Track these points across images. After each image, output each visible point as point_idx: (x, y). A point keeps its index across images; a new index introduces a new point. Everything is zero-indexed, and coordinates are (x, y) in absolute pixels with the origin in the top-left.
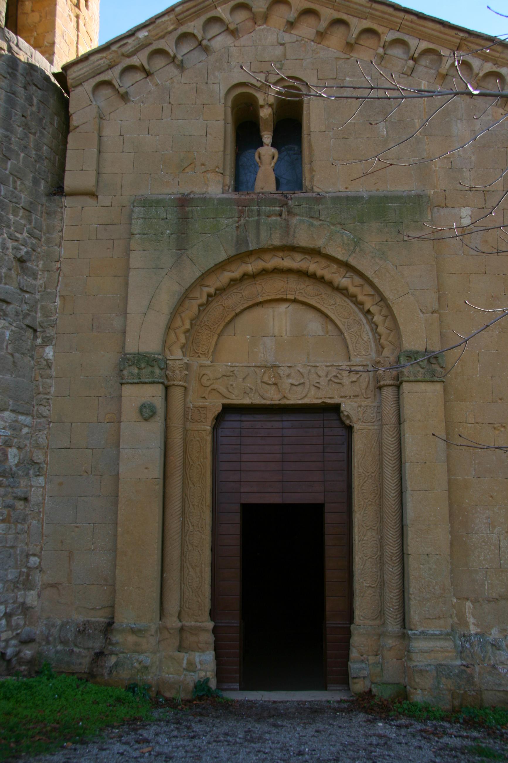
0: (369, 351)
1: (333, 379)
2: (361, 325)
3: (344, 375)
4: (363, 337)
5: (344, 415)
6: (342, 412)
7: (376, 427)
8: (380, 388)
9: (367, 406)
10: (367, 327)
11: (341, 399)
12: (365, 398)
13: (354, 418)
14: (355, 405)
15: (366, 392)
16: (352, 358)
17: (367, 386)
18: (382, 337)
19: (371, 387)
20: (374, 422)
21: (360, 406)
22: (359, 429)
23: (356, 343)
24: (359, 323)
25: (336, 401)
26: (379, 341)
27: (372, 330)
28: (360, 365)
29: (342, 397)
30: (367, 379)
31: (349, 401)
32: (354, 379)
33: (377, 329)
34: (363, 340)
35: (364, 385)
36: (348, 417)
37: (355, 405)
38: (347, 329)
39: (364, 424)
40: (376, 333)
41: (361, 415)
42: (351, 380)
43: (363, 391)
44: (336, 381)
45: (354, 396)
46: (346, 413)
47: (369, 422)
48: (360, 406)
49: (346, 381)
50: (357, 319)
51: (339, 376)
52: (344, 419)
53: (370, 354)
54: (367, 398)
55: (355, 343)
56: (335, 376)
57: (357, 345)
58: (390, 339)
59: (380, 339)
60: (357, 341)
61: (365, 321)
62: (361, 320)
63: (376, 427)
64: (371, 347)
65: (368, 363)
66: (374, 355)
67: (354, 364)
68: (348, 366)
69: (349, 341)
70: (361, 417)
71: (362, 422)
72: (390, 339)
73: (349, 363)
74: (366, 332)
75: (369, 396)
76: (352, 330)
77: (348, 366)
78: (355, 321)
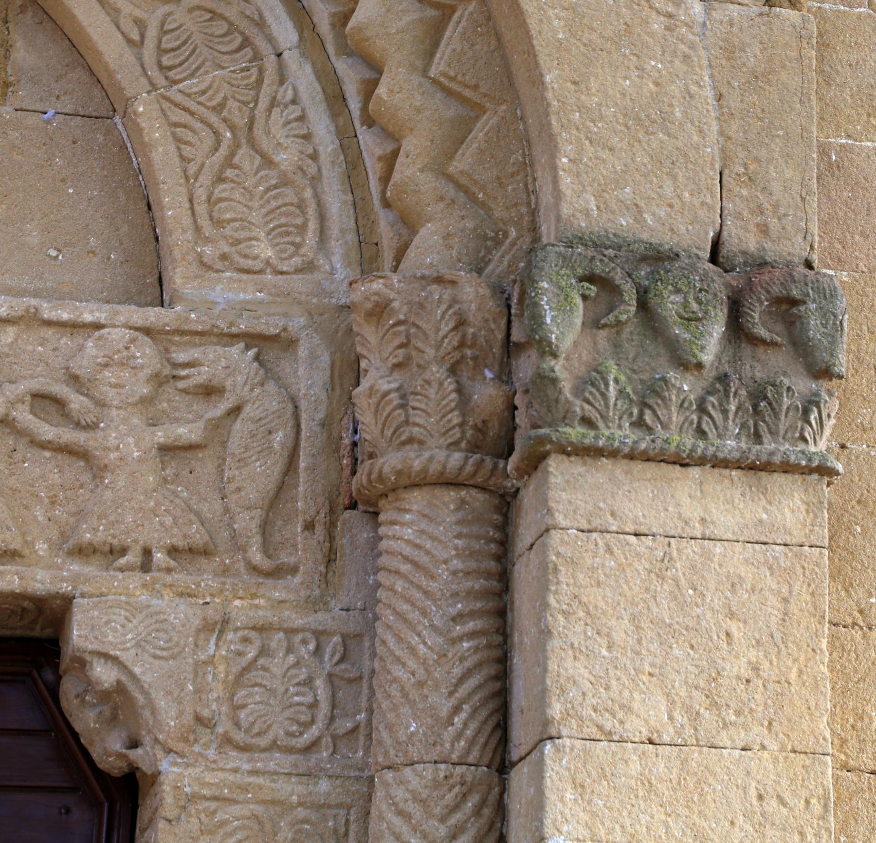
0: (311, 238)
1: (24, 416)
2: (257, 57)
3: (111, 394)
4: (266, 145)
5: (89, 684)
6: (82, 663)
7: (324, 785)
8: (368, 505)
9: (261, 629)
10: (303, 77)
11: (75, 567)
12: (254, 569)
13: (168, 715)
14: (181, 614)
15: (265, 528)
16: (179, 278)
17: (281, 488)
18: (410, 144)
19: (305, 498)
20: (313, 746)
21: (218, 626)
22: (193, 798)
23: (220, 179)
24: (247, 42)
25: (39, 580)
26: (385, 179)
27: (336, 100)
28: (235, 337)
29: (83, 552)
30: (279, 437)
31: (135, 580)
32: (186, 432)
33: (369, 88)
34: (268, 162)
35: (257, 476)
36: (119, 703)
37: (181, 614)
38: (154, 72)
39: (236, 759)
40: (369, 121)
41: (218, 690)
42: (160, 436)
43: (247, 522)
44: (48, 432)
45: (173, 551)
46: (104, 674)
47: (274, 746)
48: (218, 626)
49: (126, 440)
50: (231, 13)
51: (77, 402)
52: (85, 720)
53: (309, 267)
54: (277, 573)
55: (205, 179)
56: (38, 396)
57: (221, 190)
58: (457, 166)
59: (390, 161)
60: (229, 162)
61: (285, 32)
62: (261, 24)
63: (324, 785)
64: (322, 218)
65: (298, 322)
66: (338, 263)
67: (195, 320)
68: (147, 331)
69: (162, 157)
70: (214, 705)
71: (227, 741)
72: (457, 166)
73: (153, 315)
74: (294, 112)
75: (285, 558)
76: (191, 85)
77: (147, 331)
78: (221, 27)
